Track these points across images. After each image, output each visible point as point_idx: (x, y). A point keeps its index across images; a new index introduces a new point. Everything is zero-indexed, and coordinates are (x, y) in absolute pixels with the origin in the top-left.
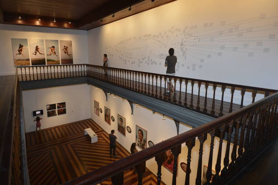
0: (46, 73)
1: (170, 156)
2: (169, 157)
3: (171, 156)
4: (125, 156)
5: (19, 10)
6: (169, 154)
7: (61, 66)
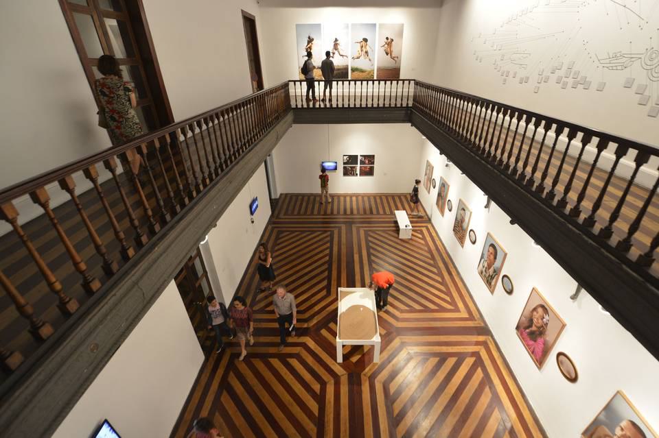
1: (539, 325)
2: (535, 326)
3: (542, 326)
6: (537, 319)
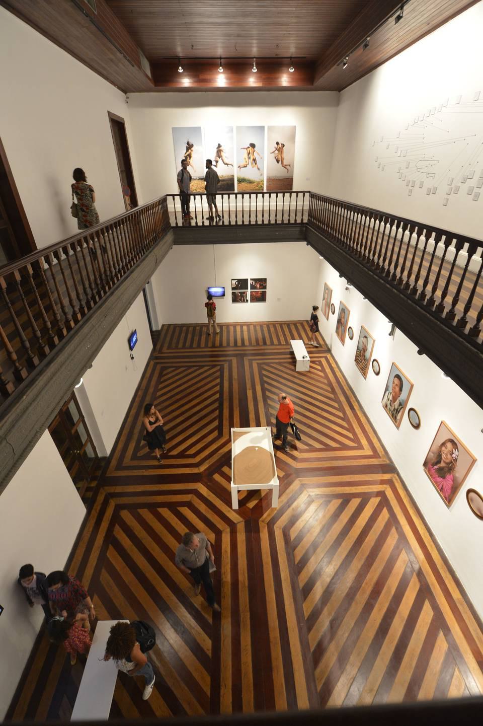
0: (198, 211)
1: (448, 461)
2: (444, 462)
3: (452, 462)
4: (90, 454)
5: (180, 51)
6: (447, 455)
7: (236, 194)
